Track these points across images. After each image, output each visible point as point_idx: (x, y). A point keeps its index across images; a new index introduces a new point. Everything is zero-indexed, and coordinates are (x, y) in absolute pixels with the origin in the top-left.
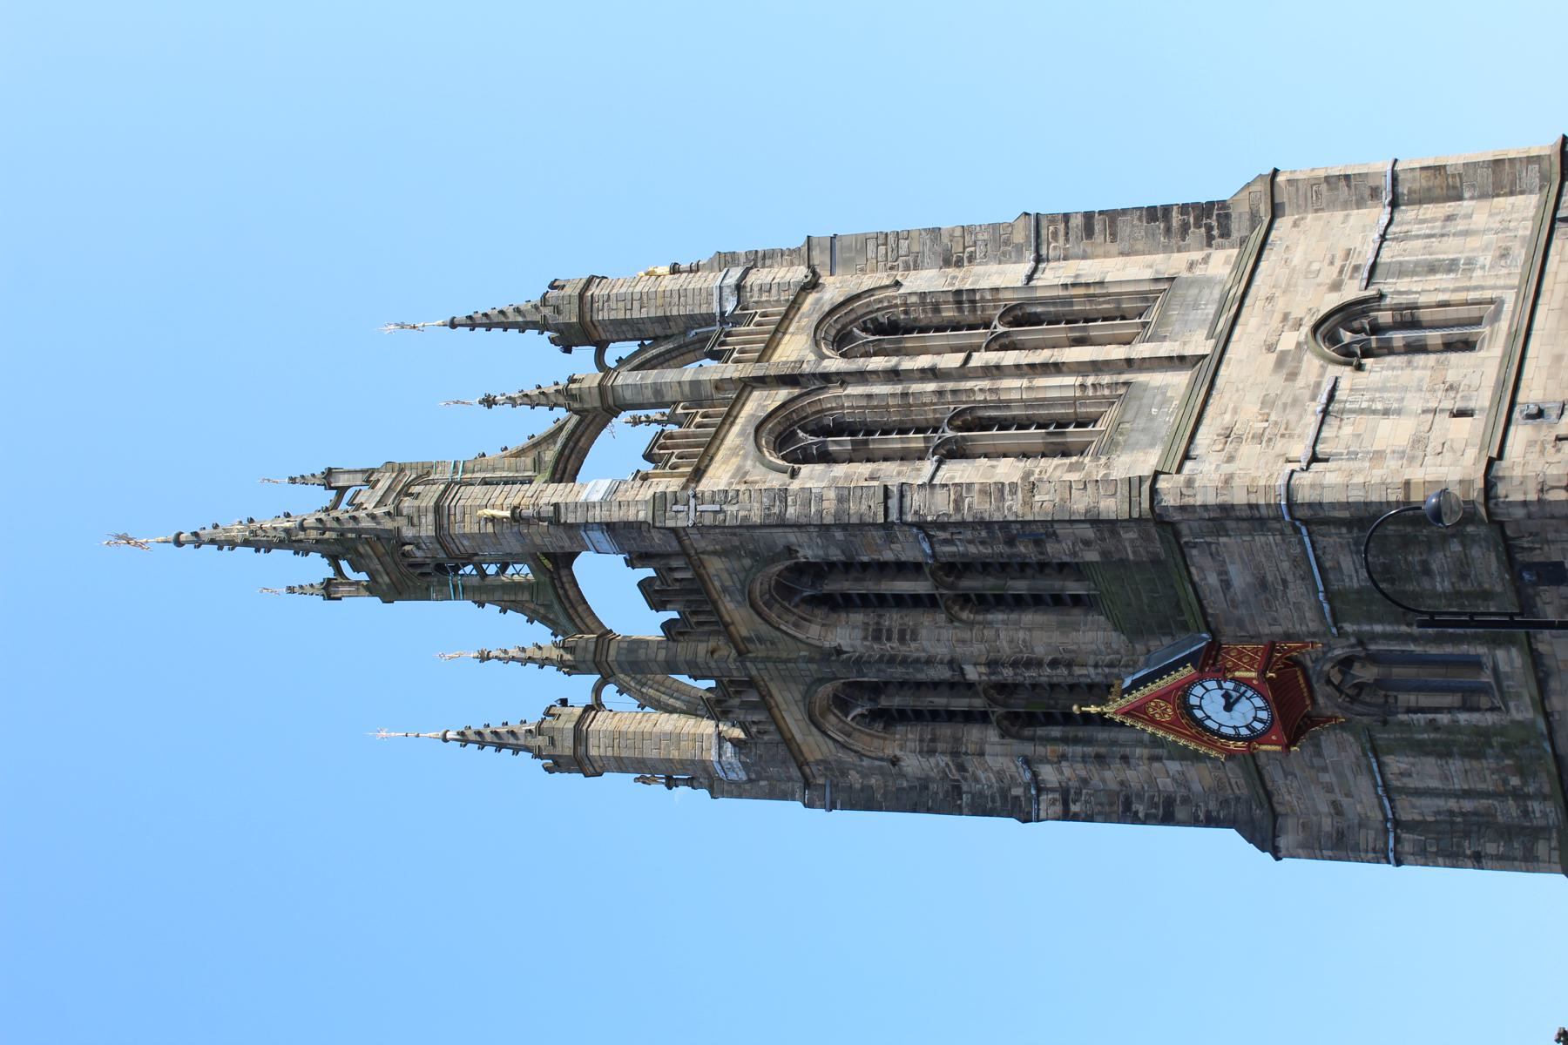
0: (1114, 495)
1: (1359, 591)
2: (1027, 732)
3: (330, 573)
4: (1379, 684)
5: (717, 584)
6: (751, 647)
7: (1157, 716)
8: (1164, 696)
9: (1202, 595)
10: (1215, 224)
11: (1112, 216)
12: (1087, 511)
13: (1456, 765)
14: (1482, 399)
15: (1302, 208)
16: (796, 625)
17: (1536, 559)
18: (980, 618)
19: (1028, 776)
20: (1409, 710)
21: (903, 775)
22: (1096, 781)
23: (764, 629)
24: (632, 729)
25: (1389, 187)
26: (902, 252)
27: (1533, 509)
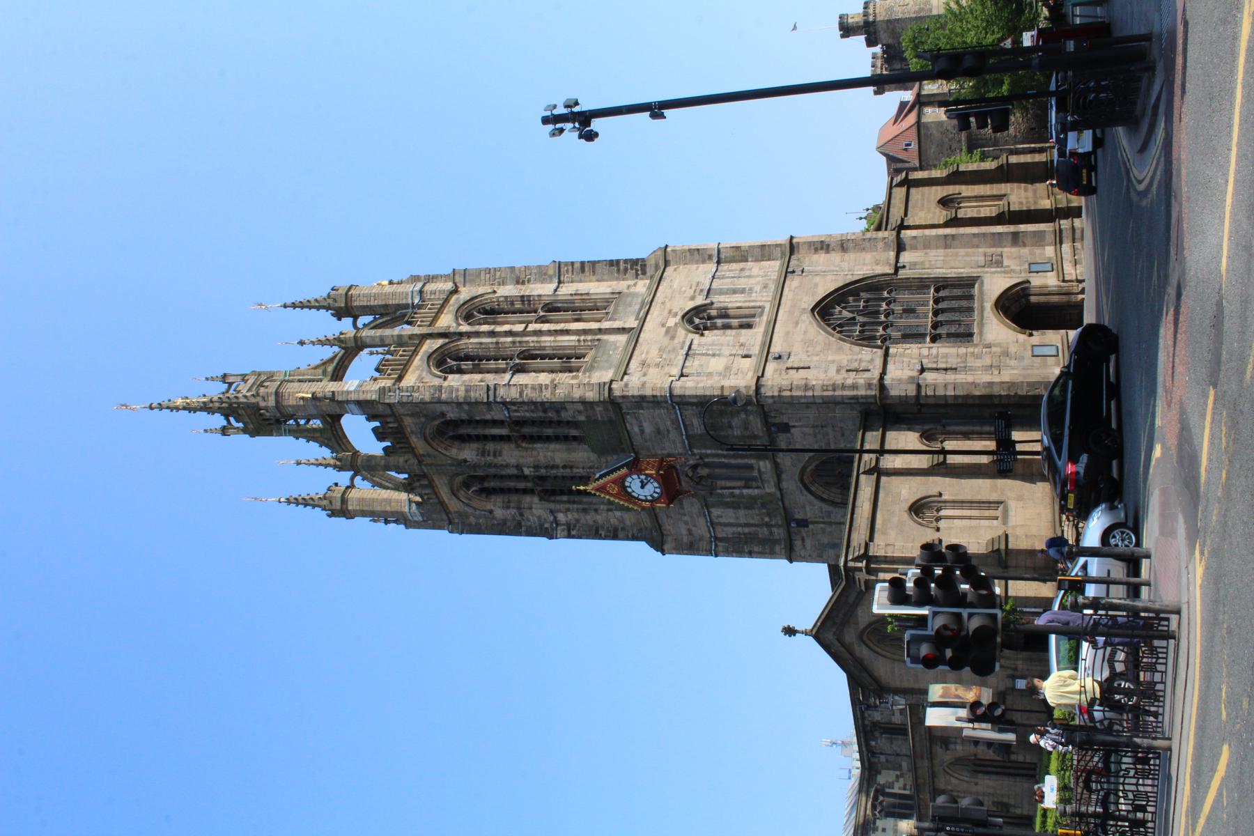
0: (592, 390)
2: (552, 498)
3: (225, 423)
4: (709, 476)
5: (409, 429)
6: (424, 459)
8: (614, 482)
10: (639, 268)
11: (593, 264)
12: (580, 397)
13: (742, 512)
14: (755, 350)
15: (678, 263)
16: (446, 449)
18: (530, 446)
19: (552, 518)
20: (722, 488)
21: (494, 518)
22: (583, 521)
23: (430, 450)
24: (368, 497)
25: (716, 255)
26: (497, 277)
27: (776, 399)
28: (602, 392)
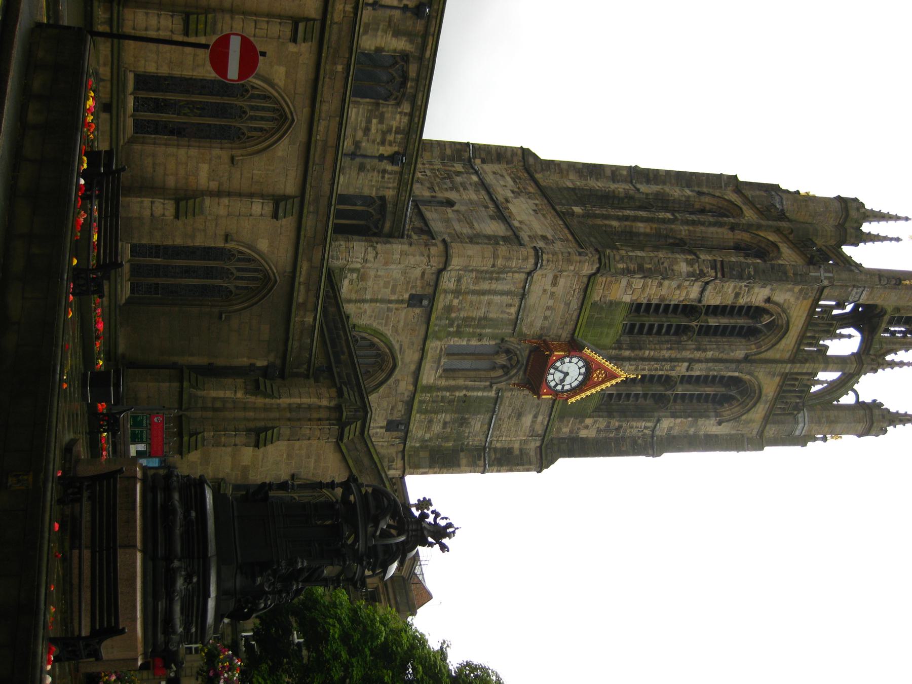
1: (479, 413)
5: (767, 406)
7: (603, 372)
9: (550, 409)
13: (481, 313)
17: (395, 433)
19: (707, 293)
28: (607, 261)
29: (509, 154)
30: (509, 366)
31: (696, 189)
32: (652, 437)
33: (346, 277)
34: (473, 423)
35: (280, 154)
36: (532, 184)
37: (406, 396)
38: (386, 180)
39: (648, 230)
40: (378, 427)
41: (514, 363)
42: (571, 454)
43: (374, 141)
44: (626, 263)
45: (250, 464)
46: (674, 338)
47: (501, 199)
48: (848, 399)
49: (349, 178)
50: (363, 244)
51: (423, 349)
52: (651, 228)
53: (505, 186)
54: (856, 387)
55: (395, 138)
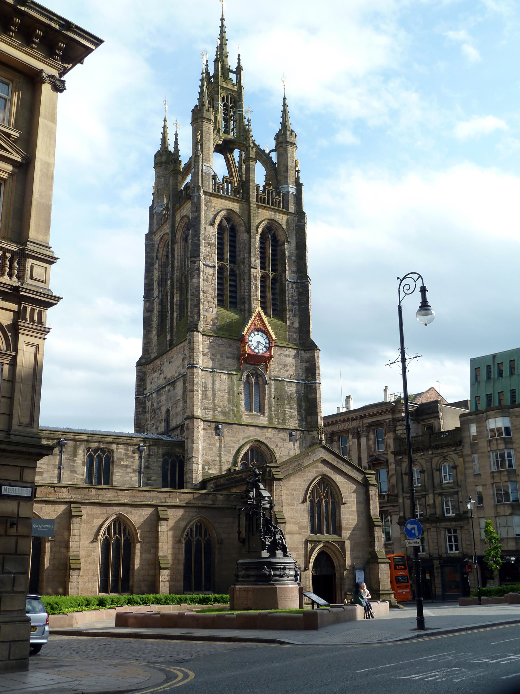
1: (284, 389)
13: (226, 395)
19: (210, 265)
29: (140, 374)
30: (256, 374)
31: (155, 260)
32: (297, 283)
33: (207, 472)
34: (290, 392)
35: (136, 519)
36: (156, 361)
37: (274, 432)
38: (153, 454)
39: (178, 295)
40: (294, 447)
41: (254, 372)
42: (308, 332)
43: (133, 462)
44: (194, 314)
45: (297, 525)
46: (238, 278)
47: (164, 382)
48: (274, 156)
49: (153, 474)
50: (188, 464)
51: (247, 425)
52: (177, 293)
53: (158, 378)
54: (267, 152)
55: (130, 451)
